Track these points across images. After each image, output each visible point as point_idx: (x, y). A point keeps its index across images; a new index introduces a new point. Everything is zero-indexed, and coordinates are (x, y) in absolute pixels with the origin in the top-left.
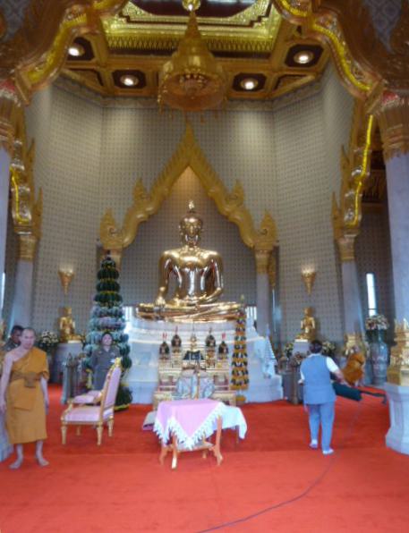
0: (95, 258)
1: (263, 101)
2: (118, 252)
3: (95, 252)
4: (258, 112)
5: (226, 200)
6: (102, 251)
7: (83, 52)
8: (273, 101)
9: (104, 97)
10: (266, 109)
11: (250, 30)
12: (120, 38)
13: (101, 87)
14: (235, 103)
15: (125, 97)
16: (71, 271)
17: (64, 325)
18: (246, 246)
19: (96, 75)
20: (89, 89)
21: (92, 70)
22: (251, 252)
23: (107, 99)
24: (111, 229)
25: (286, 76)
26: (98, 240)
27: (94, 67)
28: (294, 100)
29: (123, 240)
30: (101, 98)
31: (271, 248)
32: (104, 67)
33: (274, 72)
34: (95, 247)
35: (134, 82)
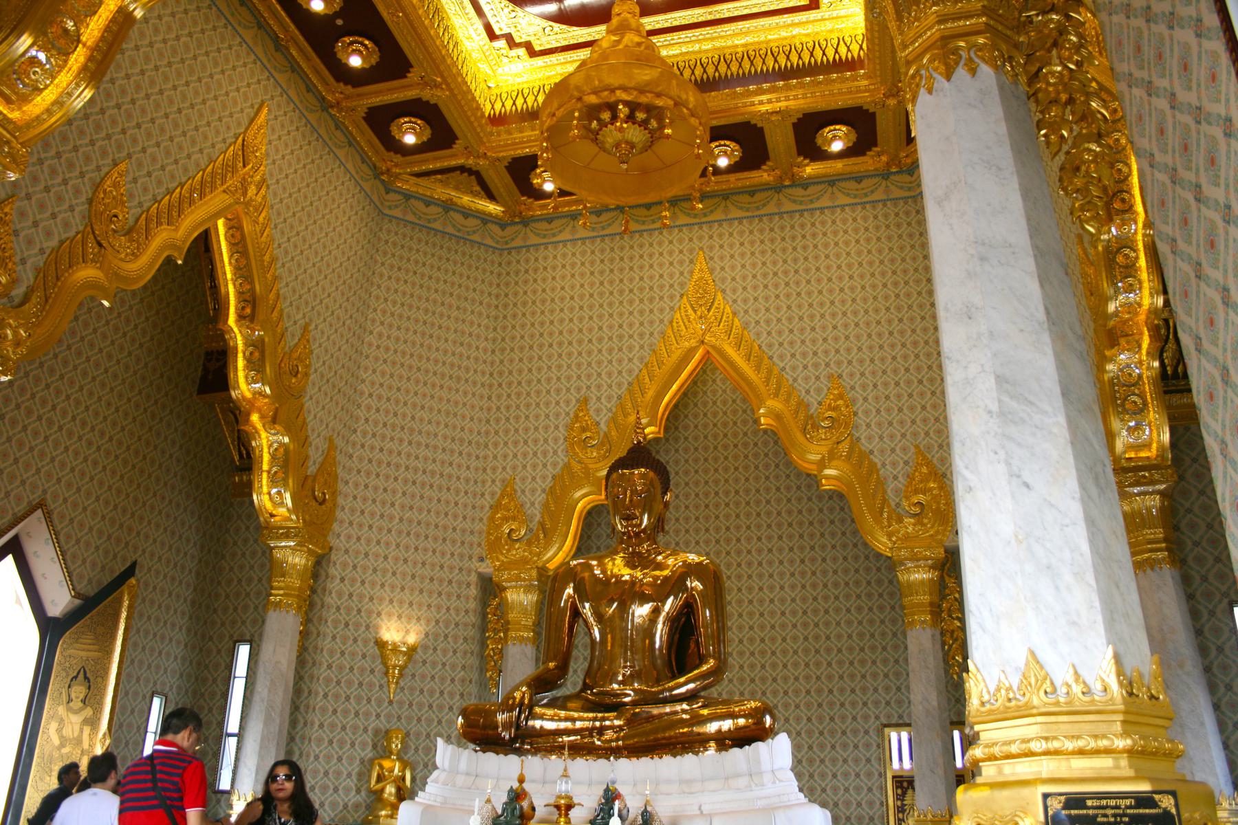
0: (472, 605)
1: (886, 176)
2: (528, 589)
3: (473, 591)
5: (804, 431)
6: (490, 589)
7: (428, 133)
9: (503, 227)
10: (897, 193)
11: (812, 15)
12: (520, 92)
14: (811, 190)
16: (412, 639)
17: (380, 778)
18: (879, 556)
19: (473, 177)
21: (462, 169)
22: (891, 565)
23: (510, 230)
24: (511, 530)
26: (481, 559)
27: (461, 161)
29: (539, 555)
30: (496, 229)
34: (473, 578)
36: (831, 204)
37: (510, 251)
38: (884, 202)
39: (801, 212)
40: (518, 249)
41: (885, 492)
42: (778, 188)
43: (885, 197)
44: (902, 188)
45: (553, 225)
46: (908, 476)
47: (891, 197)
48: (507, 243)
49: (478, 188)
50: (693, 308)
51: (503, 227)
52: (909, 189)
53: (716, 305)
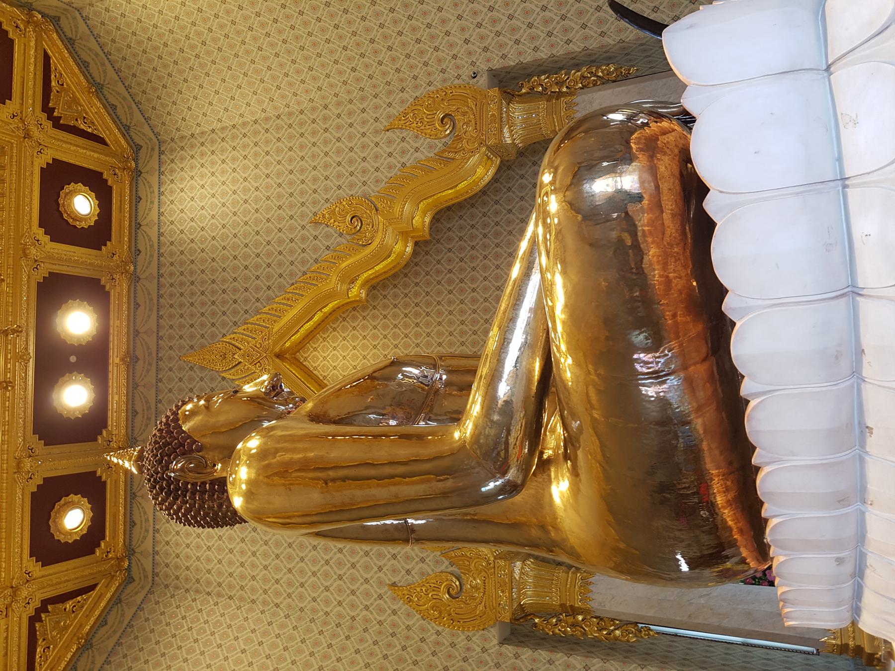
1: (136, 174)
4: (160, 184)
8: (139, 148)
10: (154, 163)
13: (93, 594)
14: (141, 247)
15: (131, 524)
20: (102, 622)
23: (135, 573)
25: (47, 110)
28: (121, 88)
30: (131, 587)
31: (495, 92)
32: (15, 590)
33: (27, 136)
35: (73, 505)
36: (156, 226)
37: (155, 574)
38: (161, 173)
39: (160, 255)
40: (154, 564)
41: (429, 159)
42: (134, 279)
43: (157, 172)
44: (151, 156)
45: (138, 521)
46: (417, 137)
47: (157, 168)
48: (146, 577)
49: (69, 605)
50: (236, 365)
51: (130, 580)
52: (153, 149)
53: (230, 341)
